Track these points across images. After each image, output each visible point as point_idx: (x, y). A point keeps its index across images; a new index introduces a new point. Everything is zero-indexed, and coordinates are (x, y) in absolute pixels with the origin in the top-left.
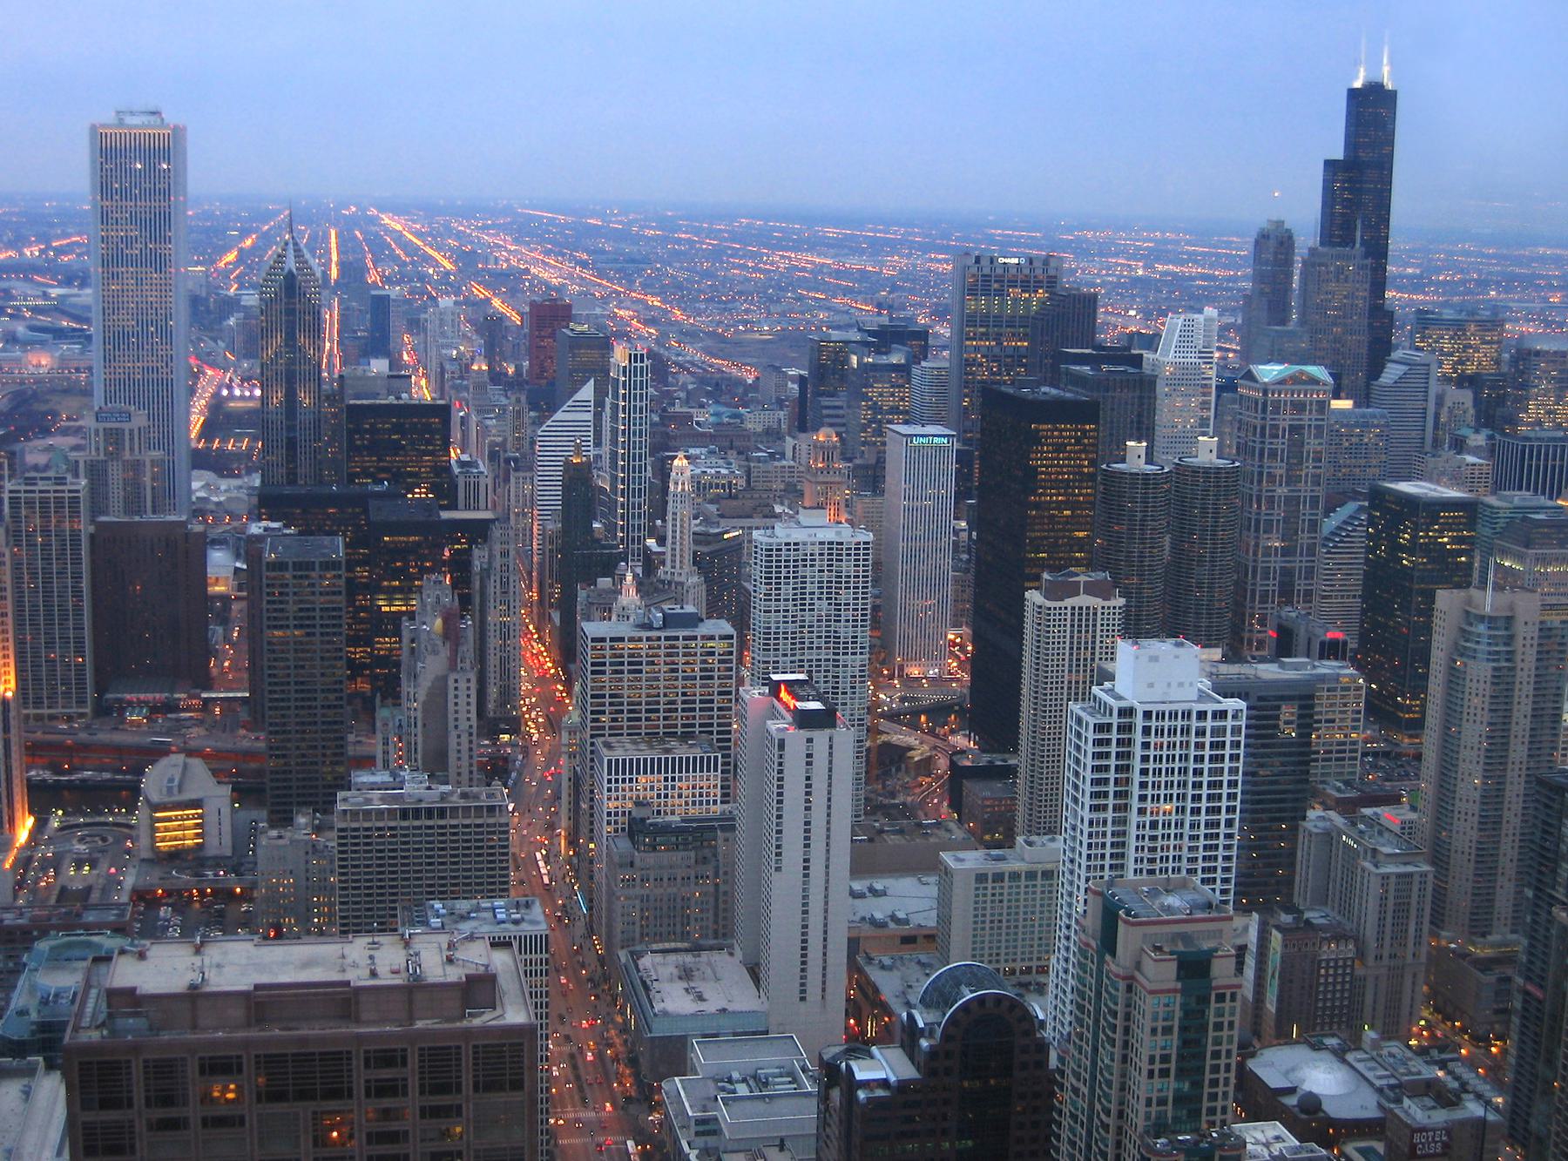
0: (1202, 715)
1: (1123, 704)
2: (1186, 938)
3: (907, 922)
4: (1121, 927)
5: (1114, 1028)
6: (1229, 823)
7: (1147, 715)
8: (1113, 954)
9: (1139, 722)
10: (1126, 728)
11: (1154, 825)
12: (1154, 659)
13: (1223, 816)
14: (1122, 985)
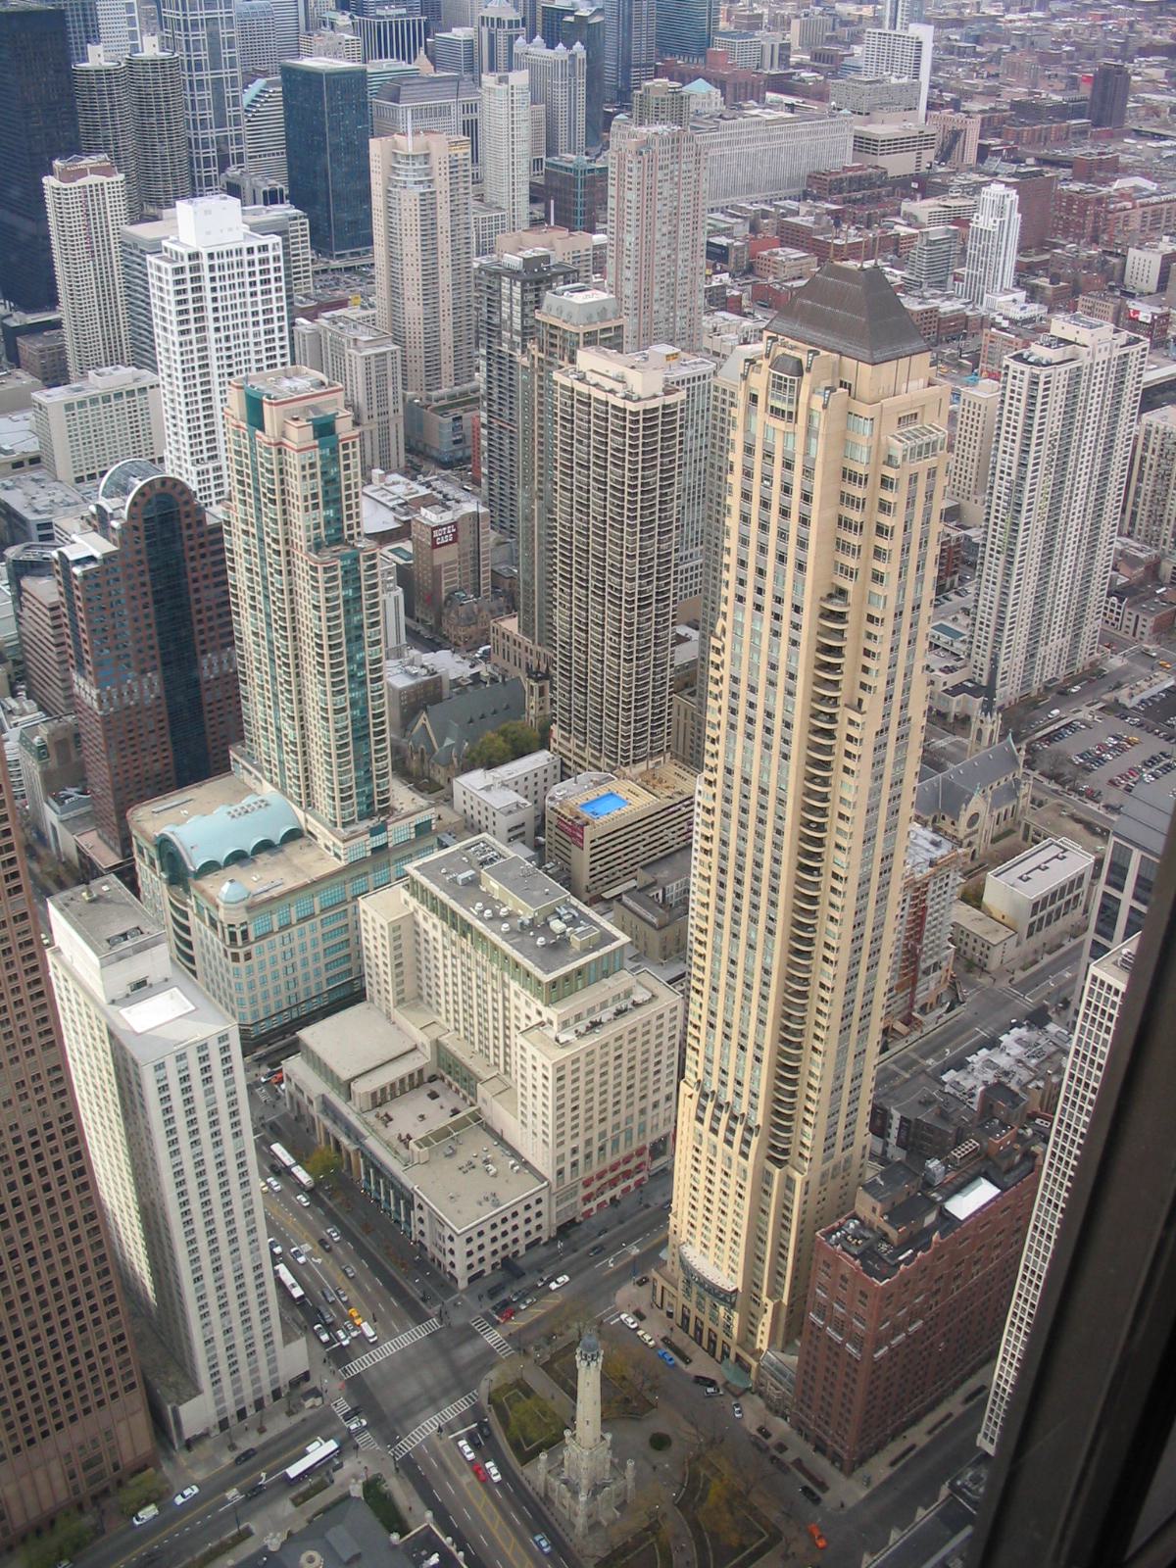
0: (250, 251)
1: (191, 251)
2: (314, 409)
3: (12, 452)
4: (266, 407)
5: (272, 482)
6: (281, 329)
7: (211, 256)
8: (262, 429)
9: (205, 262)
10: (195, 269)
11: (227, 338)
12: (207, 212)
13: (276, 325)
14: (274, 450)
